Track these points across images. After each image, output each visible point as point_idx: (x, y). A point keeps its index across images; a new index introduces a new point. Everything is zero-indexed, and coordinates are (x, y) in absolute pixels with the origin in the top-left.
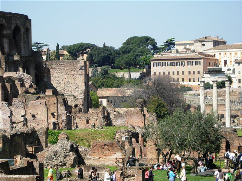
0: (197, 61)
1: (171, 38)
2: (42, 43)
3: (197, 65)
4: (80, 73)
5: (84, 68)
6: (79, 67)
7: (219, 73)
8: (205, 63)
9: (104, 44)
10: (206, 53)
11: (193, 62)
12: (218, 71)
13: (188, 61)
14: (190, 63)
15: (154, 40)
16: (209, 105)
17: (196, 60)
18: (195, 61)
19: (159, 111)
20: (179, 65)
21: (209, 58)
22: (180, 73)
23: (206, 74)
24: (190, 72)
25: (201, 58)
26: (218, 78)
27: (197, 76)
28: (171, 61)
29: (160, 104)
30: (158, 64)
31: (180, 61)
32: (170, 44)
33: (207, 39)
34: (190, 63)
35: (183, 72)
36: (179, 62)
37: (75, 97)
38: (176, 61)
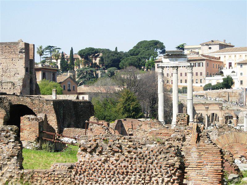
0: (200, 63)
1: (182, 44)
2: (55, 46)
3: (200, 66)
4: (19, 57)
5: (24, 51)
6: (19, 50)
7: (180, 57)
8: (207, 65)
10: (211, 56)
11: (195, 63)
12: (179, 55)
13: (191, 62)
15: (162, 43)
16: (201, 104)
17: (199, 62)
18: (198, 63)
19: (129, 105)
21: (212, 60)
23: (164, 58)
25: (204, 60)
26: (178, 63)
29: (129, 98)
33: (214, 43)
37: (14, 84)
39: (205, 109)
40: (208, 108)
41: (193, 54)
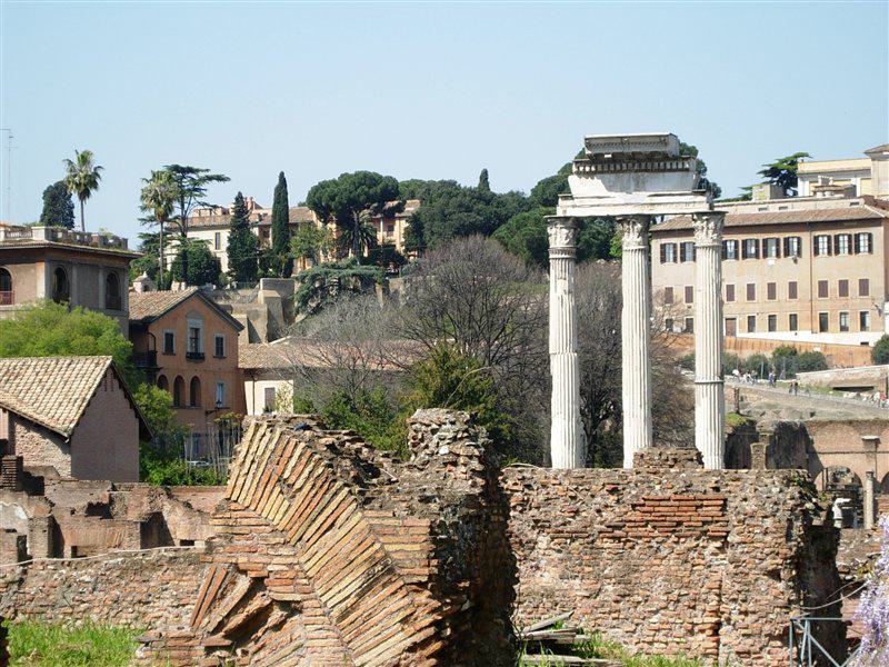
0: (857, 236)
1: (790, 154)
2: (201, 168)
3: (857, 251)
7: (659, 170)
9: (484, 176)
11: (837, 237)
12: (651, 157)
13: (817, 233)
14: (823, 244)
16: (843, 423)
17: (853, 232)
18: (850, 236)
20: (778, 255)
22: (782, 292)
23: (578, 173)
24: (823, 287)
25: (876, 221)
26: (648, 200)
27: (855, 302)
28: (740, 238)
29: (452, 387)
30: (683, 252)
31: (782, 236)
32: (784, 177)
34: (823, 244)
35: (793, 288)
36: (778, 240)
38: (761, 237)
39: (860, 446)
40: (877, 442)
41: (827, 194)
